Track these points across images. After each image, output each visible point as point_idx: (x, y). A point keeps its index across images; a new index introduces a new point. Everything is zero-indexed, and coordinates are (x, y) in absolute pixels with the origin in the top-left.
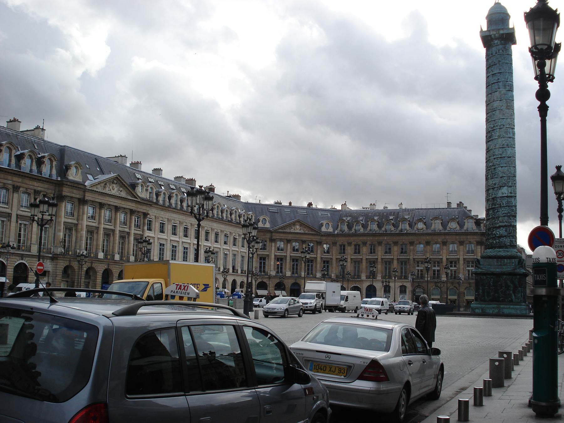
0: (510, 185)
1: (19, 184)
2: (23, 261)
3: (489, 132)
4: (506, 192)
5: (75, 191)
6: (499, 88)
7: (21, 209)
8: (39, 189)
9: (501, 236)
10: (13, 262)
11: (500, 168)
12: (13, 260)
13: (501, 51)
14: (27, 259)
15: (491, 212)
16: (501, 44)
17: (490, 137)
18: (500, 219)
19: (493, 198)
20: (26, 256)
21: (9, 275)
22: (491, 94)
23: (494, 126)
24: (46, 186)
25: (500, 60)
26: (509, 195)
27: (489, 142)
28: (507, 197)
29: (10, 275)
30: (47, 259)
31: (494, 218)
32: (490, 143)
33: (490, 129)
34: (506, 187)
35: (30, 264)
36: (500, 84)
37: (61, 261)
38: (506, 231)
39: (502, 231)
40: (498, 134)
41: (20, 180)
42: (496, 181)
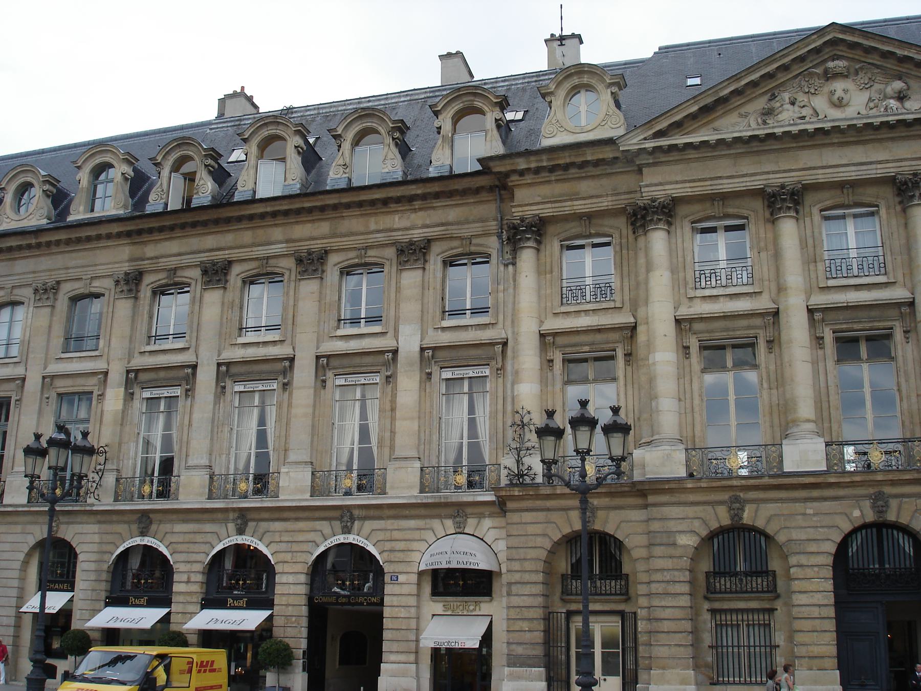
1: (317, 245)
2: (351, 539)
5: (585, 187)
7: (340, 332)
8: (417, 234)
10: (305, 547)
12: (301, 537)
14: (369, 525)
20: (363, 513)
21: (284, 600)
24: (452, 214)
29: (292, 600)
30: (481, 516)
35: (388, 546)
37: (528, 517)
41: (324, 228)
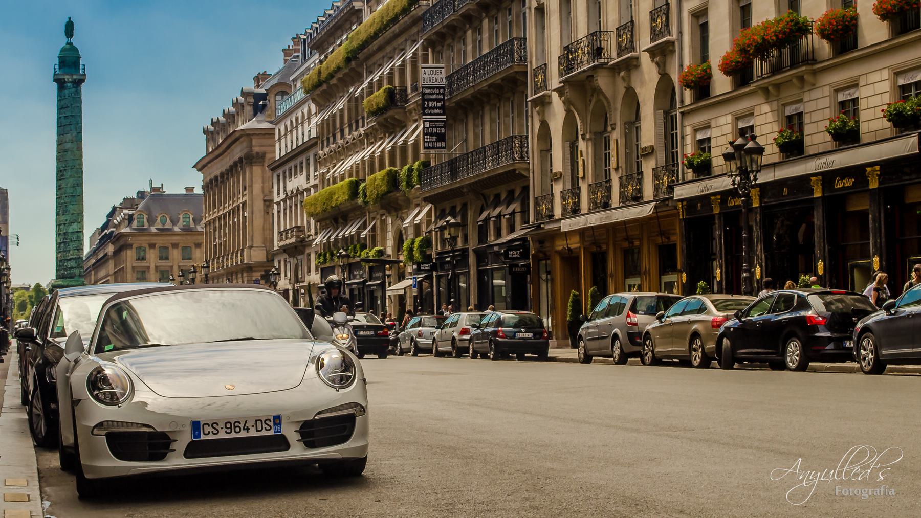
0: (79, 221)
3: (61, 171)
4: (76, 228)
6: (71, 130)
9: (72, 268)
11: (71, 206)
13: (73, 94)
15: (62, 245)
16: (74, 87)
17: (62, 176)
18: (71, 252)
19: (65, 233)
22: (63, 135)
23: (66, 166)
25: (72, 103)
26: (79, 230)
27: (61, 180)
28: (77, 232)
31: (65, 251)
32: (61, 181)
33: (62, 169)
34: (76, 223)
36: (72, 127)
38: (76, 262)
39: (73, 263)
40: (69, 174)
42: (68, 217)
